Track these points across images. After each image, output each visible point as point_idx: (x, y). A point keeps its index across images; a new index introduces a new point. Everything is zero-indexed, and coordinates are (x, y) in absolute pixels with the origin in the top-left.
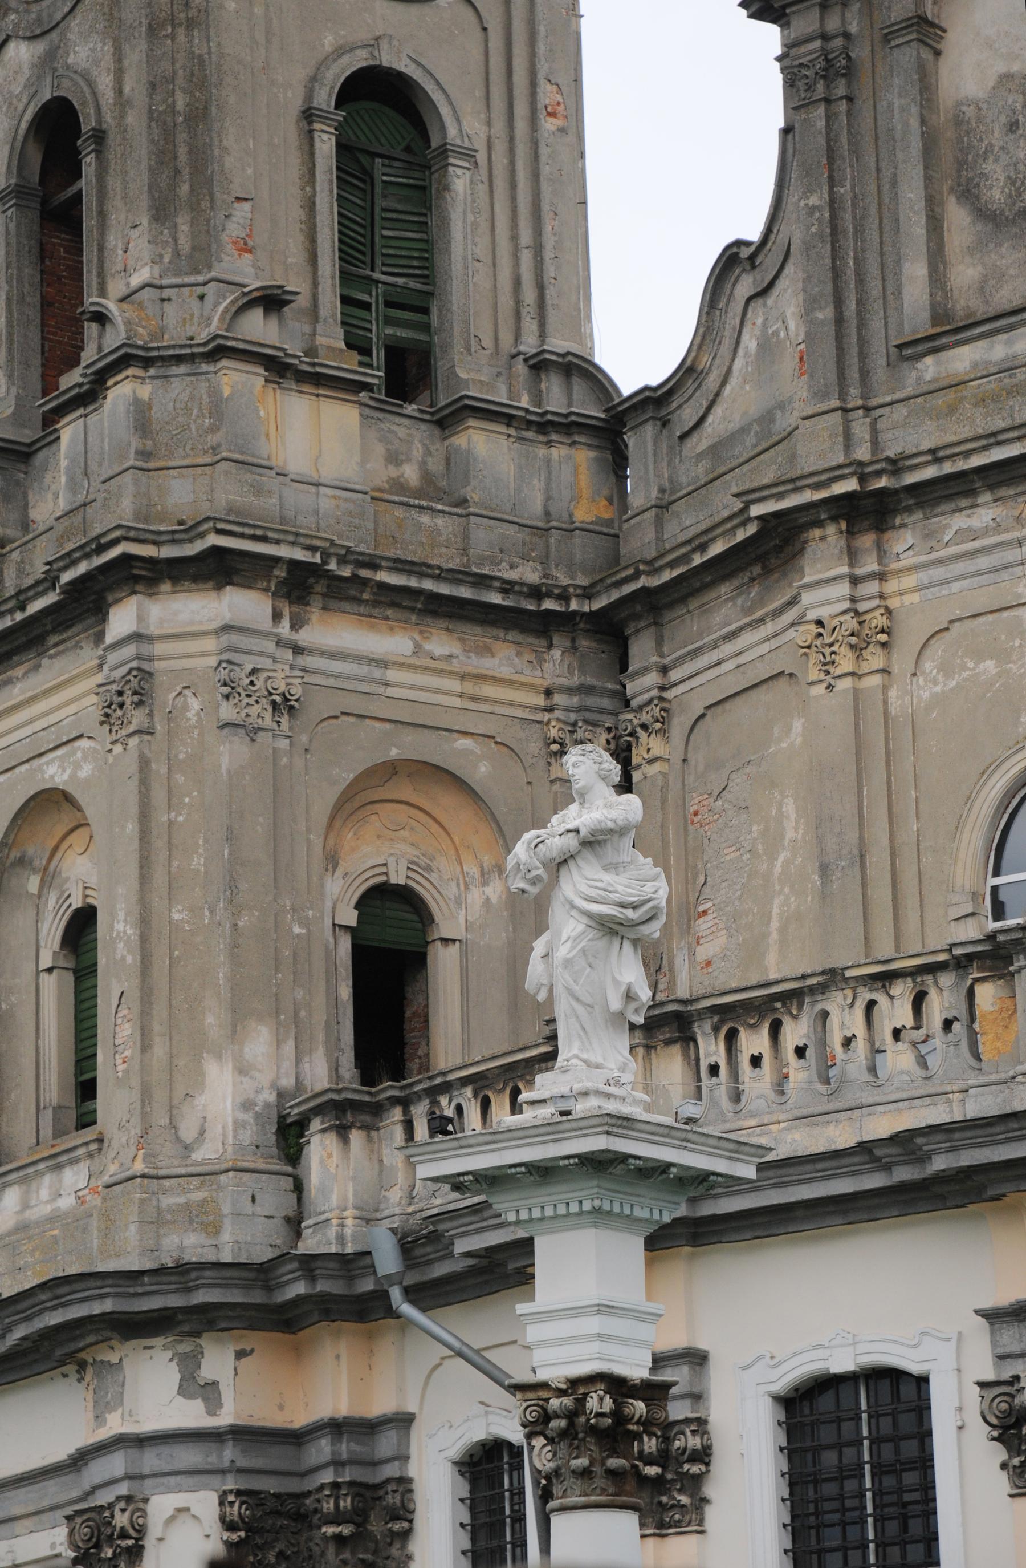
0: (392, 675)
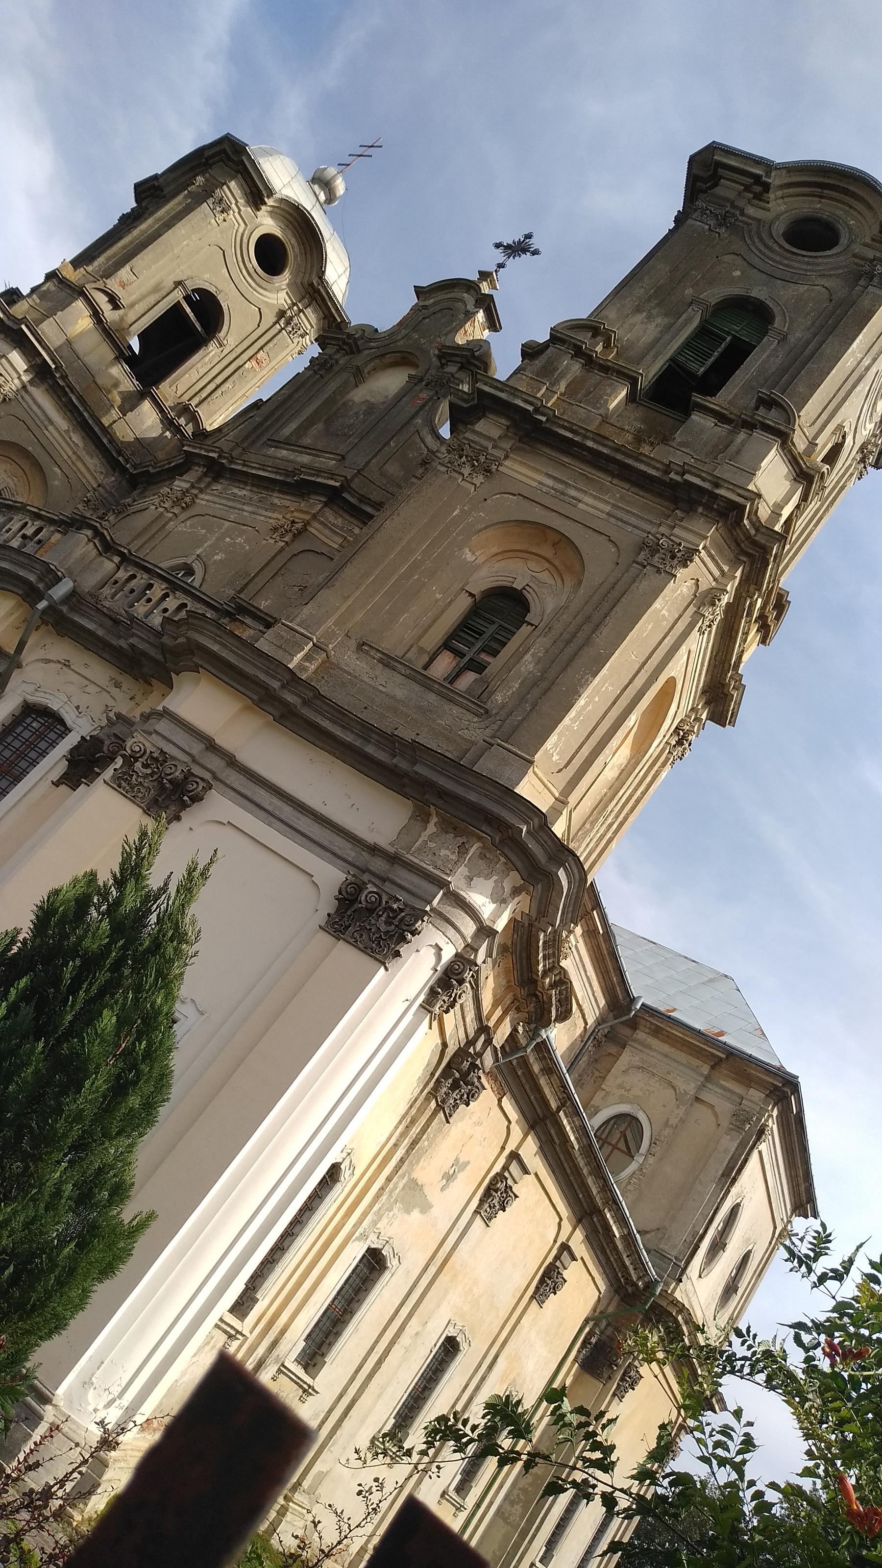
0: (51, 428)
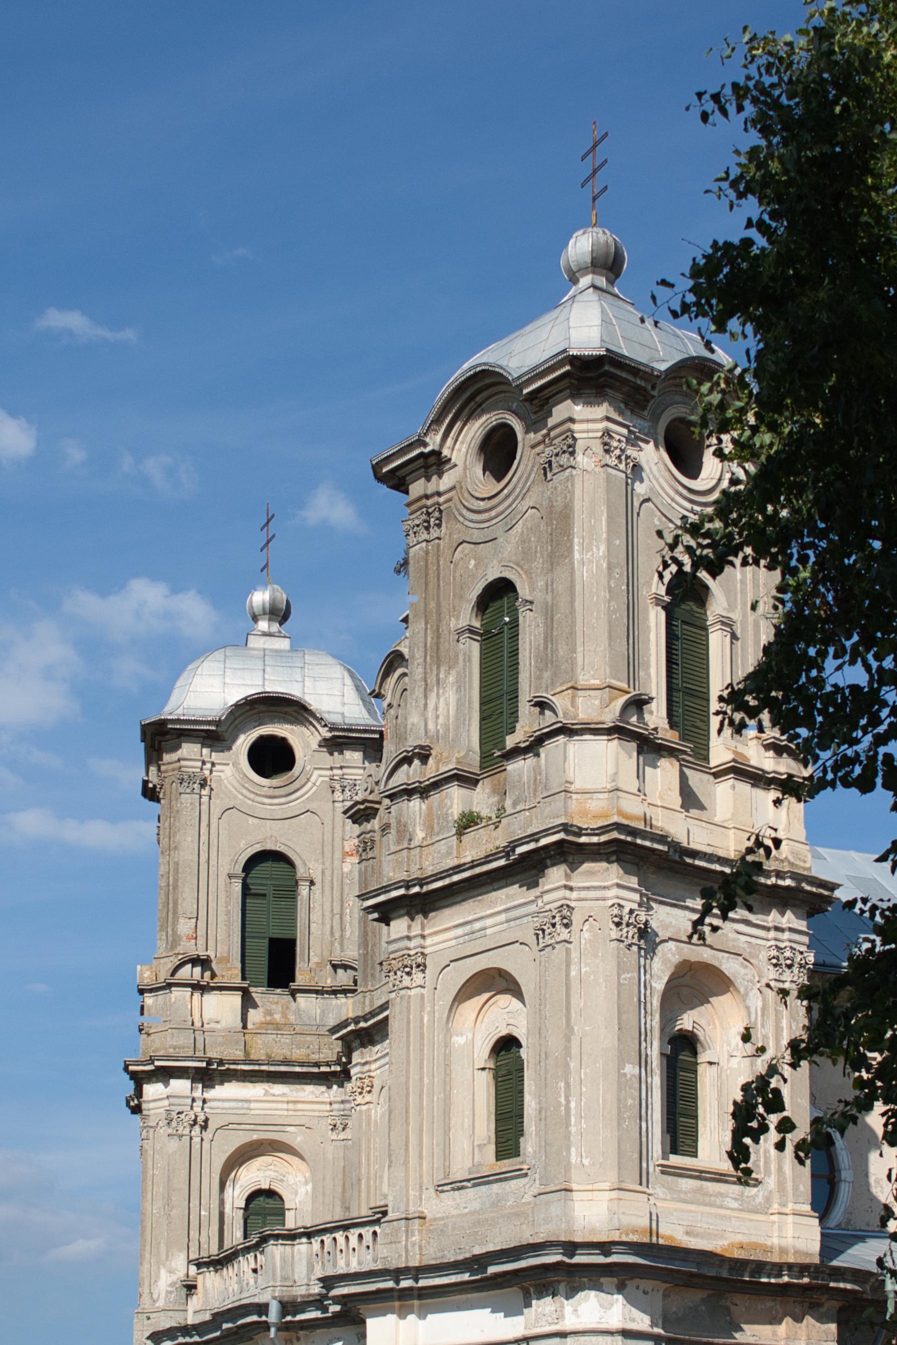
0: (253, 1105)
